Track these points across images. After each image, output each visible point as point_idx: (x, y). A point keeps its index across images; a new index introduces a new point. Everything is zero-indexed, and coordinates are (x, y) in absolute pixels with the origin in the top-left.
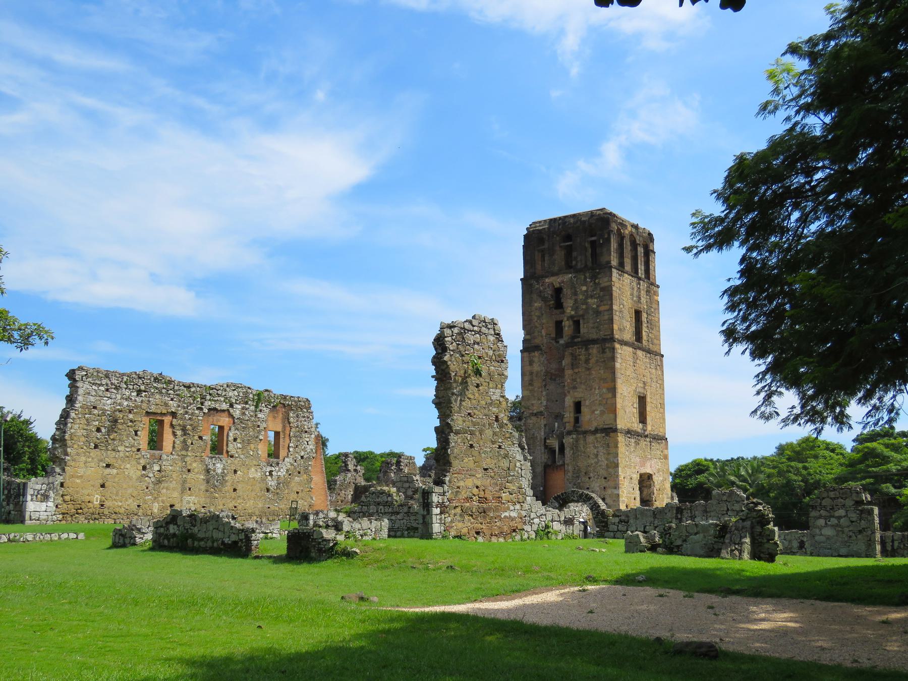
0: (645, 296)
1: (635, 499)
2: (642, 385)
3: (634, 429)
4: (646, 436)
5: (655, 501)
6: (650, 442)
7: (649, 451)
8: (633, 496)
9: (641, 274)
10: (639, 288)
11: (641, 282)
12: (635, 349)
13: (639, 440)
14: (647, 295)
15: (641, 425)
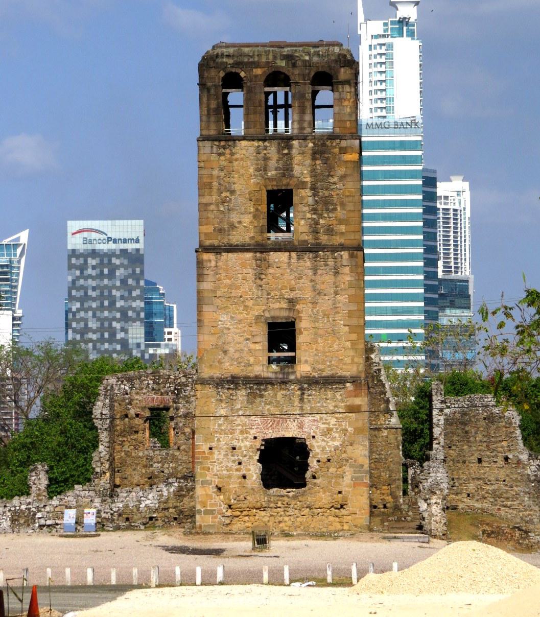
0: (308, 162)
1: (244, 477)
2: (285, 306)
3: (252, 375)
4: (284, 382)
5: (314, 477)
6: (301, 389)
7: (296, 403)
8: (242, 473)
9: (302, 128)
10: (289, 154)
11: (295, 143)
12: (262, 252)
13: (265, 390)
14: (314, 159)
15: (274, 367)
